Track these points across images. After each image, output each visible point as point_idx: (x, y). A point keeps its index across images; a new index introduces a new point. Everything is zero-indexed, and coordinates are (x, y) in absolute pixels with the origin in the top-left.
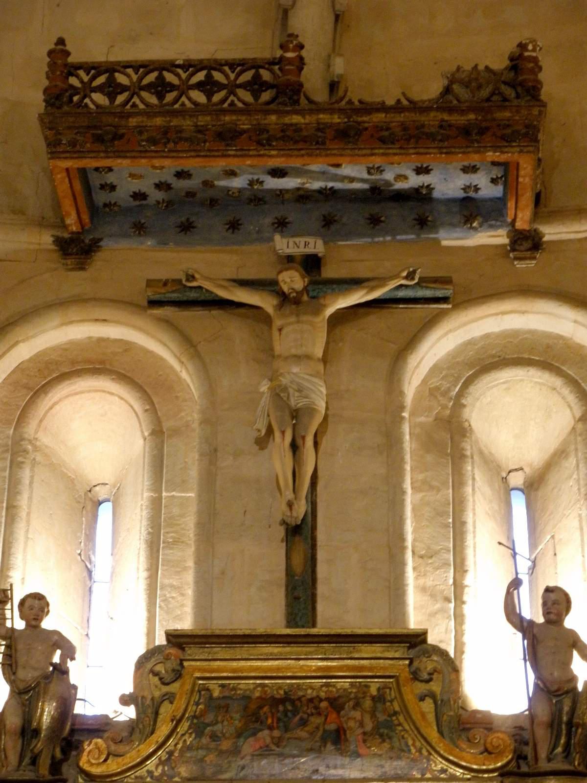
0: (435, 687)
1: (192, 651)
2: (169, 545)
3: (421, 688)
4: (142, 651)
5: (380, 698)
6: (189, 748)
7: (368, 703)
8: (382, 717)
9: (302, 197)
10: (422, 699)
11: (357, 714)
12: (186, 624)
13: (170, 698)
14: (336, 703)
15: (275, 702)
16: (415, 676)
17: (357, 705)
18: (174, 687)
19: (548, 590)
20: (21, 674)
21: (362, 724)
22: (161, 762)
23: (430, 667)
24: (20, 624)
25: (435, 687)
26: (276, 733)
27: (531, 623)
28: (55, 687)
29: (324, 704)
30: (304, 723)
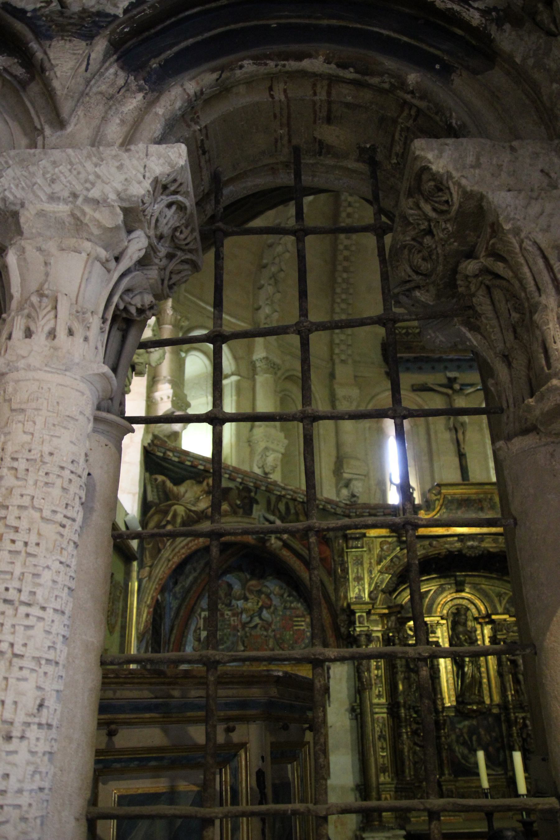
1: (442, 488)
7: (488, 500)
9: (451, 360)
13: (438, 500)
14: (480, 501)
30: (473, 506)
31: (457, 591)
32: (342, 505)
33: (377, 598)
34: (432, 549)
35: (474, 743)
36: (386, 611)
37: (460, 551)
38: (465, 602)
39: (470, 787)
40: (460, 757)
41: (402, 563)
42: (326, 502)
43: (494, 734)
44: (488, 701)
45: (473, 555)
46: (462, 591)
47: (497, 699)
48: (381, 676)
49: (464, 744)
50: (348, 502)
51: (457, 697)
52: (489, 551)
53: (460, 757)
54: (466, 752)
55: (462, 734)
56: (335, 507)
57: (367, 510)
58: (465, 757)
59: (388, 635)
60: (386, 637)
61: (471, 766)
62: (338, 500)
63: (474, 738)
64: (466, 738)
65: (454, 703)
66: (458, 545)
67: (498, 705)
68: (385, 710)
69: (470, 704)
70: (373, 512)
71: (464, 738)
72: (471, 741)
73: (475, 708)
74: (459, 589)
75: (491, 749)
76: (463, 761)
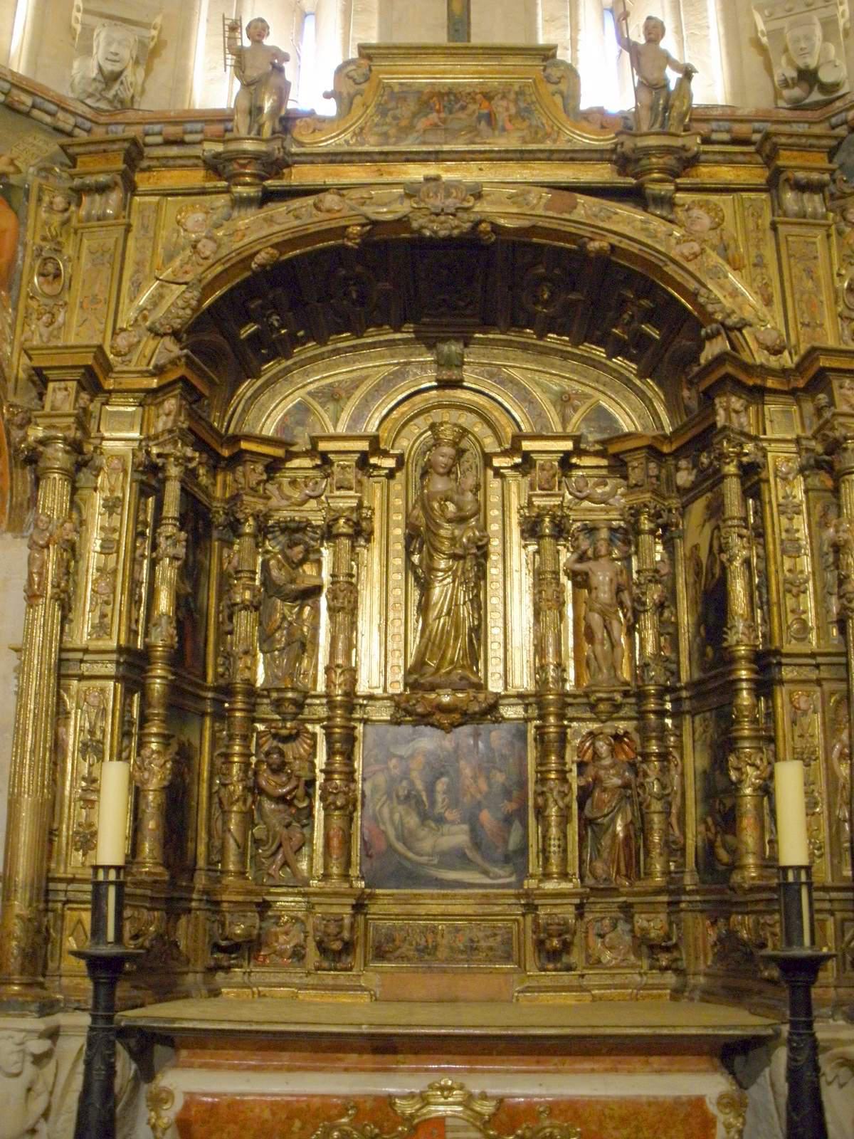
0: (563, 87)
2: (357, 12)
3: (552, 88)
4: (340, 62)
5: (520, 93)
6: (377, 125)
7: (512, 96)
8: (522, 105)
10: (553, 95)
11: (504, 103)
12: (373, 38)
13: (359, 93)
15: (441, 95)
16: (548, 80)
17: (504, 97)
18: (365, 86)
19: (649, 18)
20: (248, 72)
21: (507, 109)
22: (355, 134)
23: (559, 74)
24: (247, 43)
25: (563, 87)
26: (443, 115)
27: (635, 44)
28: (274, 80)
29: (479, 97)
30: (463, 108)
31: (444, 385)
32: (81, 109)
33: (132, 347)
34: (322, 216)
35: (439, 798)
36: (154, 383)
37: (402, 222)
38: (466, 419)
39: (410, 916)
40: (391, 833)
41: (224, 252)
42: (13, 85)
43: (499, 778)
44: (495, 686)
45: (443, 233)
46: (457, 384)
47: (523, 680)
48: (115, 571)
49: (410, 799)
50: (103, 105)
51: (408, 673)
52: (496, 228)
53: (391, 833)
54: (412, 821)
55: (406, 775)
56: (52, 108)
57: (157, 128)
58: (406, 838)
59: (148, 453)
60: (142, 456)
61: (424, 859)
62: (71, 95)
63: (441, 785)
64: (420, 785)
65: (399, 689)
66: (403, 208)
67: (521, 696)
68: (111, 669)
69: (433, 688)
70: (172, 131)
71: (412, 783)
72: (431, 790)
73: (446, 699)
74: (446, 374)
75: (486, 817)
76: (399, 846)
